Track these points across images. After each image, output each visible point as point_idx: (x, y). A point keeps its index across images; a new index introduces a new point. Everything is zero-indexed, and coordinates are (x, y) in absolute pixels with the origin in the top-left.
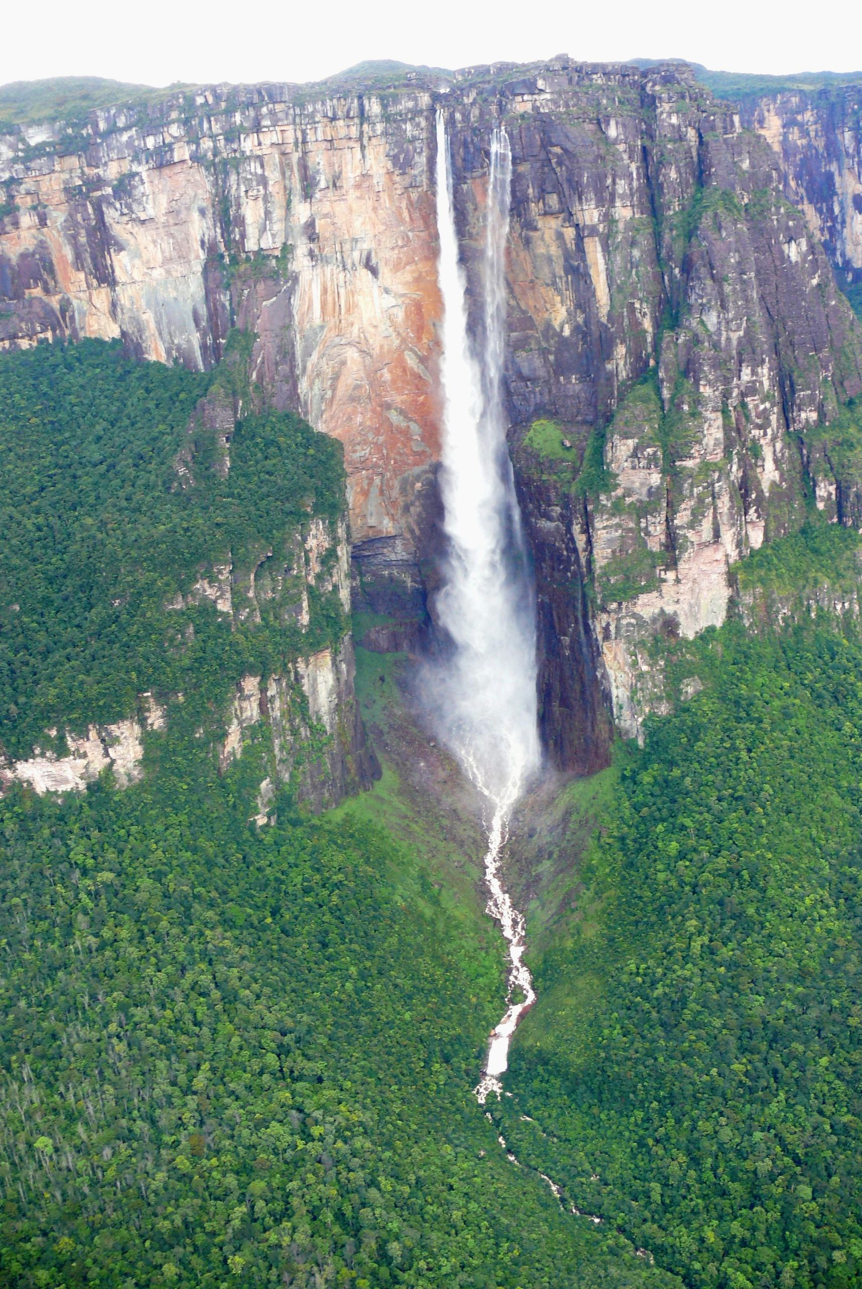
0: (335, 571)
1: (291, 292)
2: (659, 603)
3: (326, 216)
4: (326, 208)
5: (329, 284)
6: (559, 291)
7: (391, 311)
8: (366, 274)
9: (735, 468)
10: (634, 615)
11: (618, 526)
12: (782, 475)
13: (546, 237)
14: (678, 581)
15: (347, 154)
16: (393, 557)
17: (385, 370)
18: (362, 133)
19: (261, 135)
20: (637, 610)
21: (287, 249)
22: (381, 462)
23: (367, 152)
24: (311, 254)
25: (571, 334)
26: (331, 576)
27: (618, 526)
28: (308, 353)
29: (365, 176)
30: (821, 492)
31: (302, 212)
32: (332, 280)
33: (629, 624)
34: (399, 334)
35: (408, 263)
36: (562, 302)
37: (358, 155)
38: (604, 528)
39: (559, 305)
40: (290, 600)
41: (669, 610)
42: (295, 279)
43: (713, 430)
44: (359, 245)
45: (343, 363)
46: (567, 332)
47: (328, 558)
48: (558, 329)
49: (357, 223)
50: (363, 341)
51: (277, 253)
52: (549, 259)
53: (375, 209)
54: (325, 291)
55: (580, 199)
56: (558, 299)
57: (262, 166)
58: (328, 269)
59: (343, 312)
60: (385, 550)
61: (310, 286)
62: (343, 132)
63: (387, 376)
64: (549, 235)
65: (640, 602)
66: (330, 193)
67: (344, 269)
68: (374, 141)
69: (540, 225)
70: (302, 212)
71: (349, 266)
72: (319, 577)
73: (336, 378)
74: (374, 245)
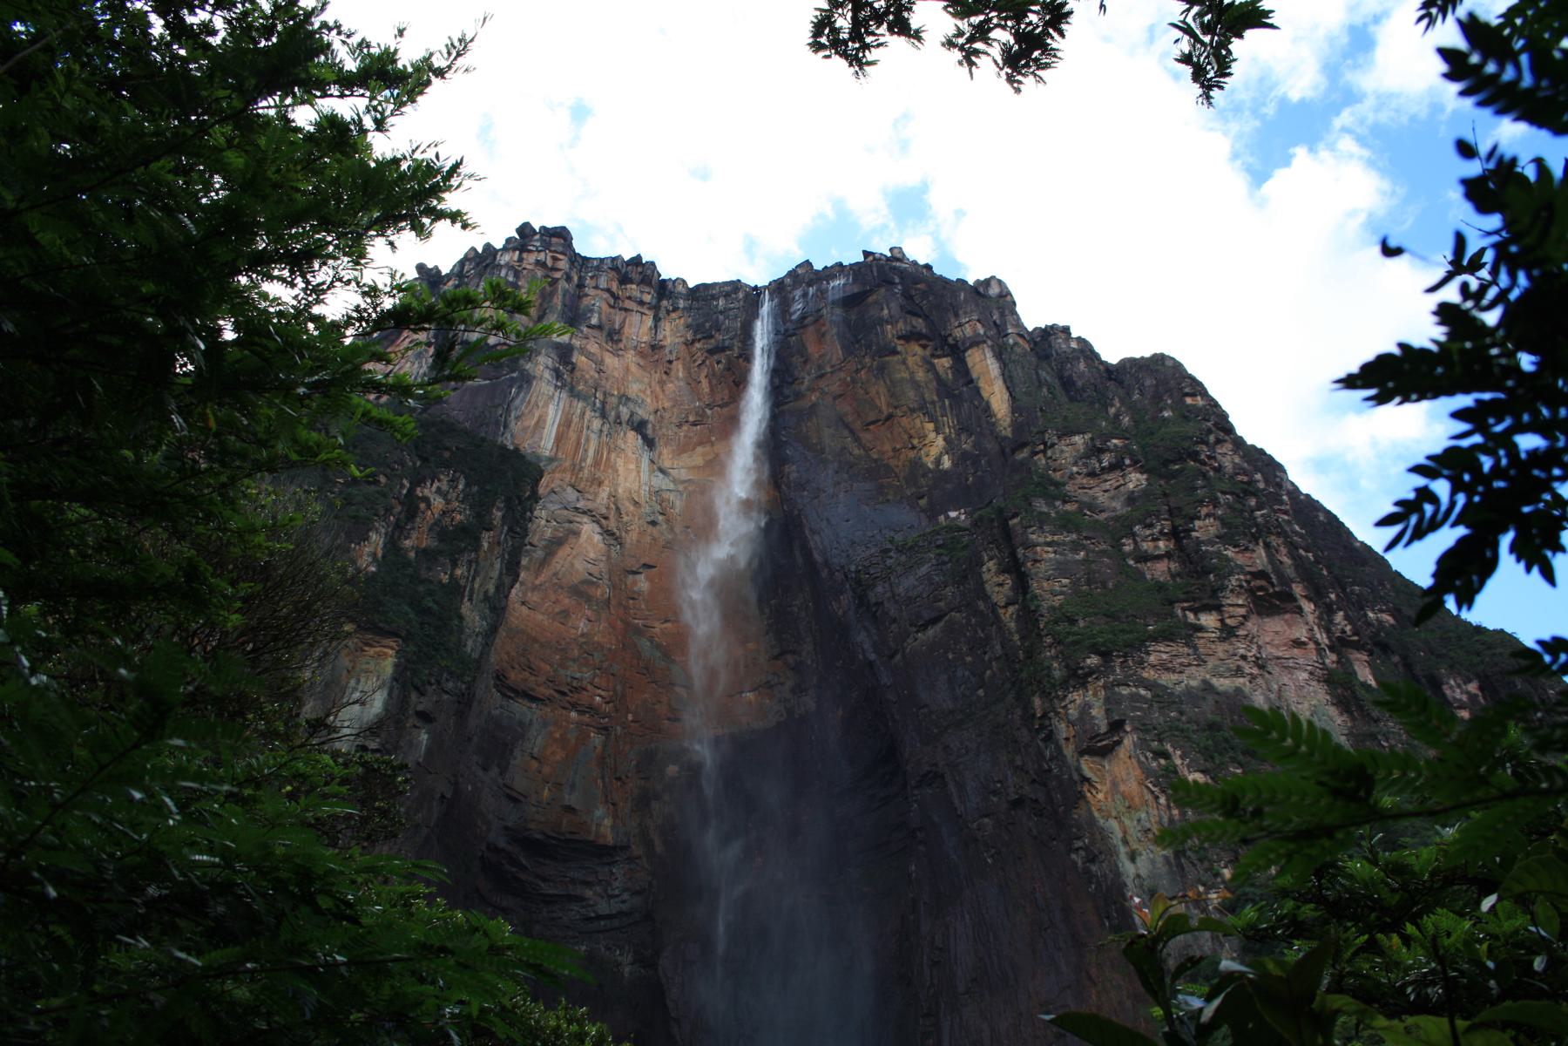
0: (466, 557)
3: (589, 356)
5: (575, 419)
6: (932, 419)
7: (666, 495)
13: (910, 360)
16: (603, 907)
17: (642, 577)
19: (525, 255)
22: (607, 708)
23: (662, 324)
25: (954, 464)
27: (1076, 546)
29: (655, 347)
33: (1135, 698)
34: (672, 530)
35: (701, 443)
36: (937, 431)
37: (649, 322)
38: (1049, 544)
39: (932, 435)
41: (1223, 684)
42: (526, 380)
44: (631, 405)
46: (947, 463)
48: (931, 466)
50: (612, 516)
52: (916, 385)
54: (566, 423)
55: (957, 316)
56: (931, 426)
58: (579, 406)
59: (589, 461)
60: (589, 893)
63: (642, 583)
65: (1152, 658)
67: (604, 416)
68: (673, 315)
69: (899, 348)
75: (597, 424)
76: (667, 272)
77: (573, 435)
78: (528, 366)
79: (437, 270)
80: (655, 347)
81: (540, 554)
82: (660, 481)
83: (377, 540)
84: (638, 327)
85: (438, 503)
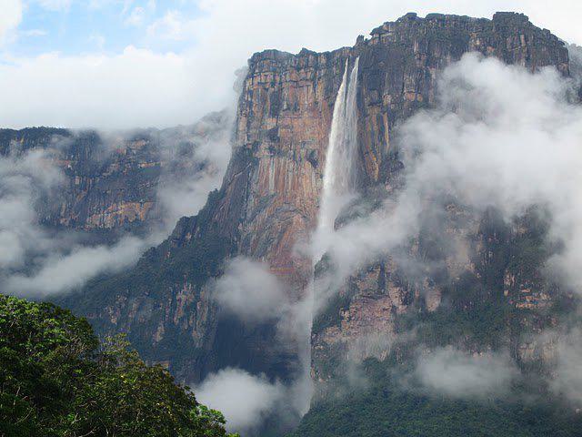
1: (252, 169)
2: (340, 336)
4: (288, 121)
8: (308, 165)
10: (324, 344)
14: (350, 318)
15: (305, 88)
18: (315, 76)
20: (326, 339)
21: (256, 145)
24: (271, 149)
26: (189, 320)
28: (258, 210)
30: (508, 283)
31: (270, 123)
32: (284, 166)
40: (152, 325)
41: (344, 339)
42: (256, 162)
44: (306, 146)
45: (291, 223)
51: (250, 147)
53: (320, 124)
54: (278, 173)
57: (252, 97)
58: (282, 160)
61: (268, 170)
62: (303, 76)
66: (290, 113)
70: (270, 123)
71: (298, 159)
72: (182, 320)
73: (284, 231)
74: (318, 147)
75: (291, 166)
76: (319, 49)
80: (316, 103)
81: (276, 241)
83: (161, 329)
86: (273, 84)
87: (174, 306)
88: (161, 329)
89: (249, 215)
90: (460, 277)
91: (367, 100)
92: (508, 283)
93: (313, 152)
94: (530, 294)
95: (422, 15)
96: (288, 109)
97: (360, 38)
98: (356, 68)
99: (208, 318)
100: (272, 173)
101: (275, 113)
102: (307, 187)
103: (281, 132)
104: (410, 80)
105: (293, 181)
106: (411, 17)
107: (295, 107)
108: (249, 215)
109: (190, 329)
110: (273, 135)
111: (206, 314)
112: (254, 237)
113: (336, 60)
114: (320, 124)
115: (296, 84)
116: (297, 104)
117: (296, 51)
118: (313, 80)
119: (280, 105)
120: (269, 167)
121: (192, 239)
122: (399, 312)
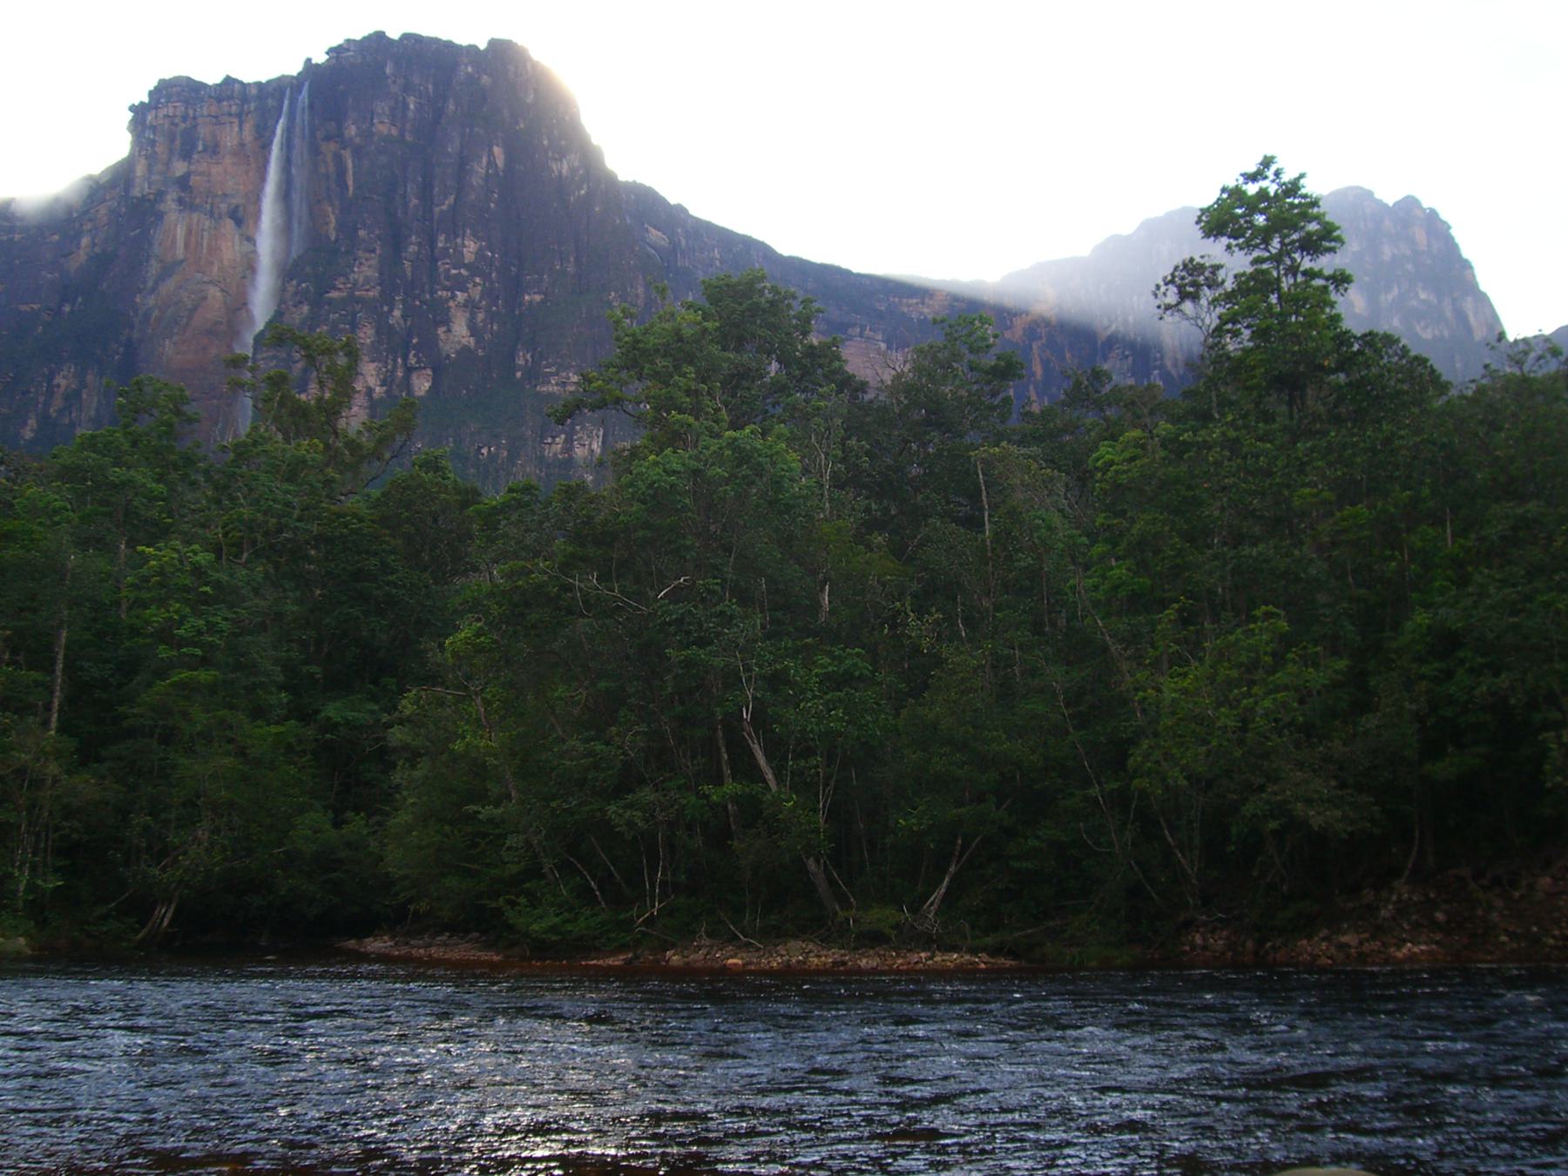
3: (201, 174)
4: (203, 167)
8: (229, 224)
9: (397, 313)
11: (275, 357)
12: (477, 342)
15: (228, 128)
21: (160, 195)
24: (180, 201)
27: (275, 357)
28: (161, 278)
29: (242, 145)
30: (521, 362)
42: (160, 216)
43: (364, 268)
45: (205, 298)
47: (73, 398)
49: (230, 183)
54: (189, 232)
58: (195, 216)
62: (226, 109)
64: (329, 158)
67: (211, 214)
70: (180, 168)
72: (61, 412)
73: (195, 308)
75: (207, 223)
77: (193, 239)
78: (162, 207)
79: (142, 103)
80: (242, 145)
82: (247, 247)
83: (32, 422)
84: (229, 138)
85: (63, 382)
86: (184, 118)
87: (50, 392)
88: (32, 422)
89: (150, 284)
90: (457, 352)
91: (319, 135)
92: (521, 362)
93: (237, 207)
94: (557, 374)
95: (394, 34)
96: (205, 150)
97: (309, 60)
98: (305, 92)
99: (97, 410)
100: (180, 233)
101: (186, 155)
102: (231, 249)
103: (194, 180)
104: (382, 107)
105: (209, 245)
106: (380, 36)
107: (214, 149)
108: (150, 284)
109: (72, 425)
110: (183, 183)
111: (94, 405)
112: (156, 313)
113: (272, 95)
114: (247, 172)
115: (217, 120)
116: (217, 145)
117: (218, 80)
118: (239, 115)
119: (194, 146)
120: (176, 228)
121: (72, 312)
122: (375, 396)
